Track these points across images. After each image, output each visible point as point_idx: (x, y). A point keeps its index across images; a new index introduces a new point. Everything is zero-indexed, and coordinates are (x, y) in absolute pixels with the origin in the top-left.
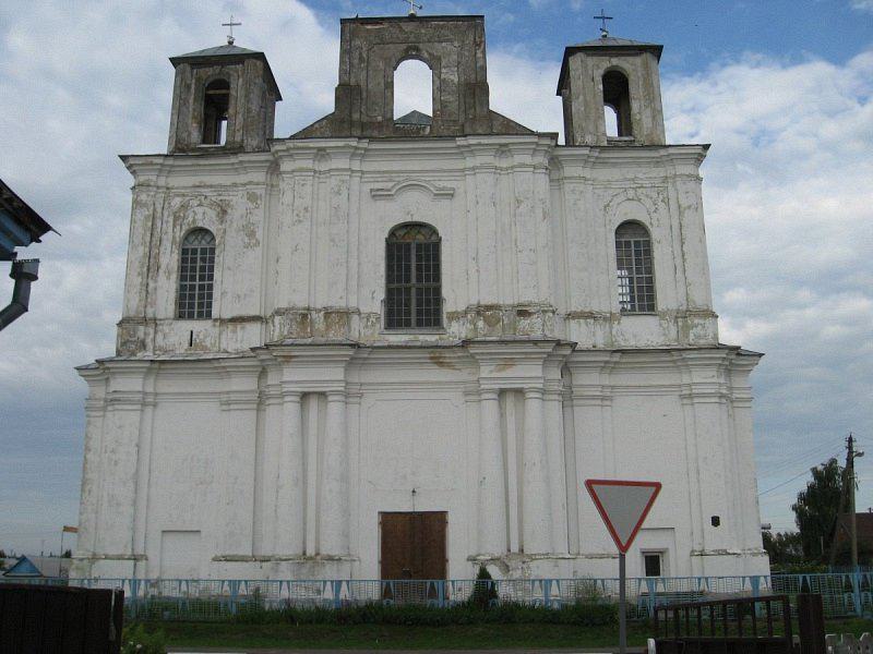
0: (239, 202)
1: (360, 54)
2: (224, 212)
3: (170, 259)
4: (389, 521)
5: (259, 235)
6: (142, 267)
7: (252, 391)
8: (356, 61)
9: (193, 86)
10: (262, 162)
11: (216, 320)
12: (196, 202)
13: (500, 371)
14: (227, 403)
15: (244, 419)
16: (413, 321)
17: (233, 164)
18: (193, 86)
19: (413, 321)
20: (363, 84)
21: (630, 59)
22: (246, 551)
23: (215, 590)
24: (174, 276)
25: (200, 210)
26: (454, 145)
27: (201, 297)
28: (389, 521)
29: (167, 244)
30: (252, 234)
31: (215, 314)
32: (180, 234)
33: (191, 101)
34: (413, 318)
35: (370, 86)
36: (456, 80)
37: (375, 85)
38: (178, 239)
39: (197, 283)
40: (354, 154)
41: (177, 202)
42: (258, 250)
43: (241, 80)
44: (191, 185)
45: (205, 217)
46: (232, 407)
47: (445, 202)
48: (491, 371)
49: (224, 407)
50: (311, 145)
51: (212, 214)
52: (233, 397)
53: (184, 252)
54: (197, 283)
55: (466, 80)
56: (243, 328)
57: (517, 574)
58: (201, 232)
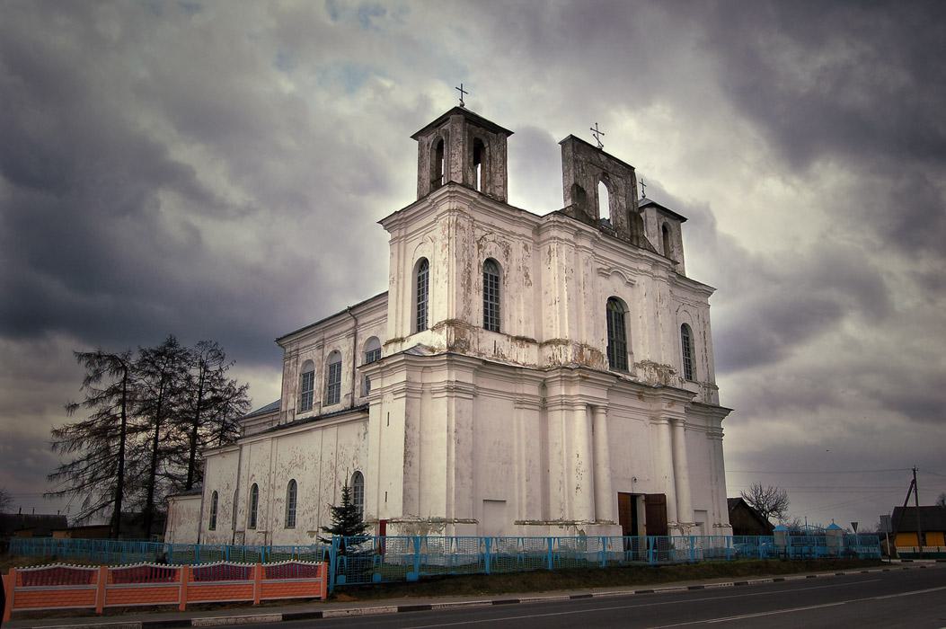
0: (517, 248)
3: (478, 278)
4: (622, 496)
6: (464, 280)
7: (537, 396)
10: (533, 222)
13: (670, 407)
14: (520, 403)
15: (528, 418)
17: (514, 217)
22: (538, 518)
23: (521, 547)
25: (494, 245)
26: (428, 204)
28: (622, 496)
37: (589, 192)
40: (595, 241)
41: (479, 233)
42: (531, 288)
45: (498, 255)
46: (523, 406)
47: (629, 289)
49: (518, 405)
50: (578, 226)
51: (501, 250)
52: (526, 398)
56: (528, 347)
57: (686, 534)
58: (491, 262)
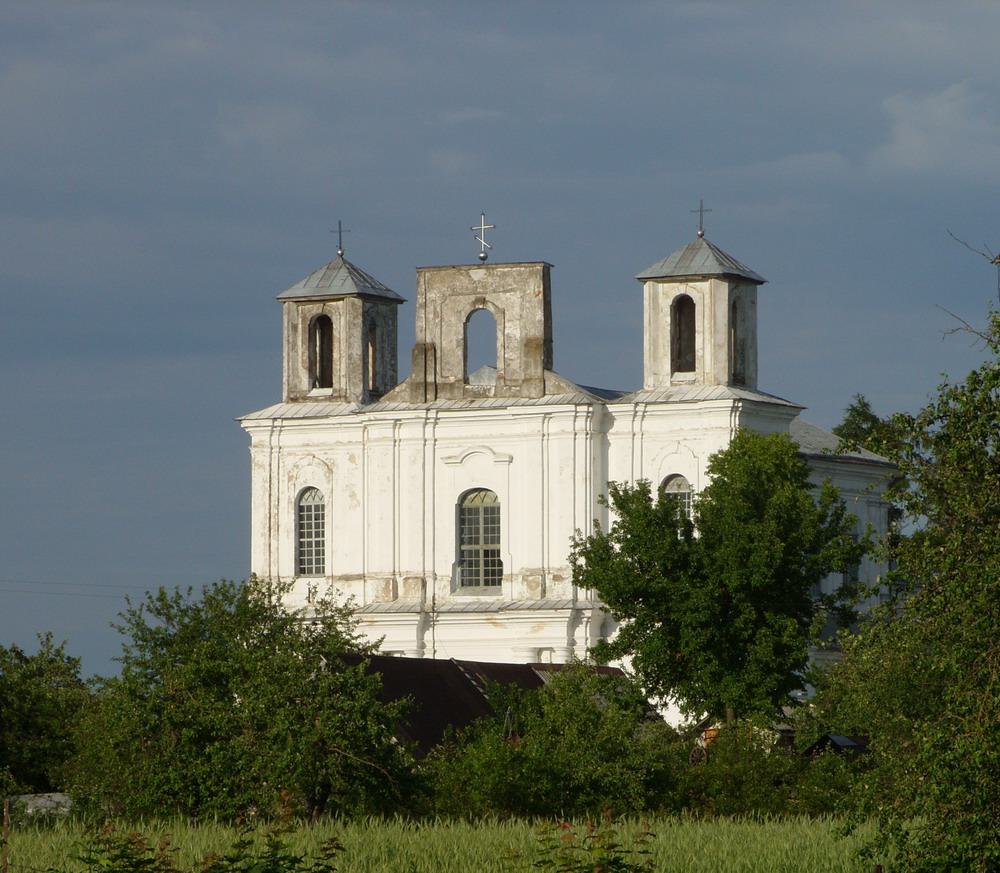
1: (435, 308)
2: (330, 471)
5: (359, 497)
8: (431, 316)
9: (300, 326)
11: (328, 577)
12: (305, 462)
16: (482, 582)
18: (300, 326)
19: (482, 582)
20: (437, 342)
21: (698, 284)
24: (292, 535)
27: (318, 553)
29: (284, 504)
30: (353, 495)
31: (328, 572)
32: (294, 494)
33: (300, 343)
34: (482, 578)
35: (444, 343)
36: (518, 336)
38: (293, 500)
39: (314, 539)
43: (343, 319)
44: (301, 443)
48: (527, 633)
51: (321, 471)
53: (300, 509)
54: (314, 539)
55: (526, 335)
